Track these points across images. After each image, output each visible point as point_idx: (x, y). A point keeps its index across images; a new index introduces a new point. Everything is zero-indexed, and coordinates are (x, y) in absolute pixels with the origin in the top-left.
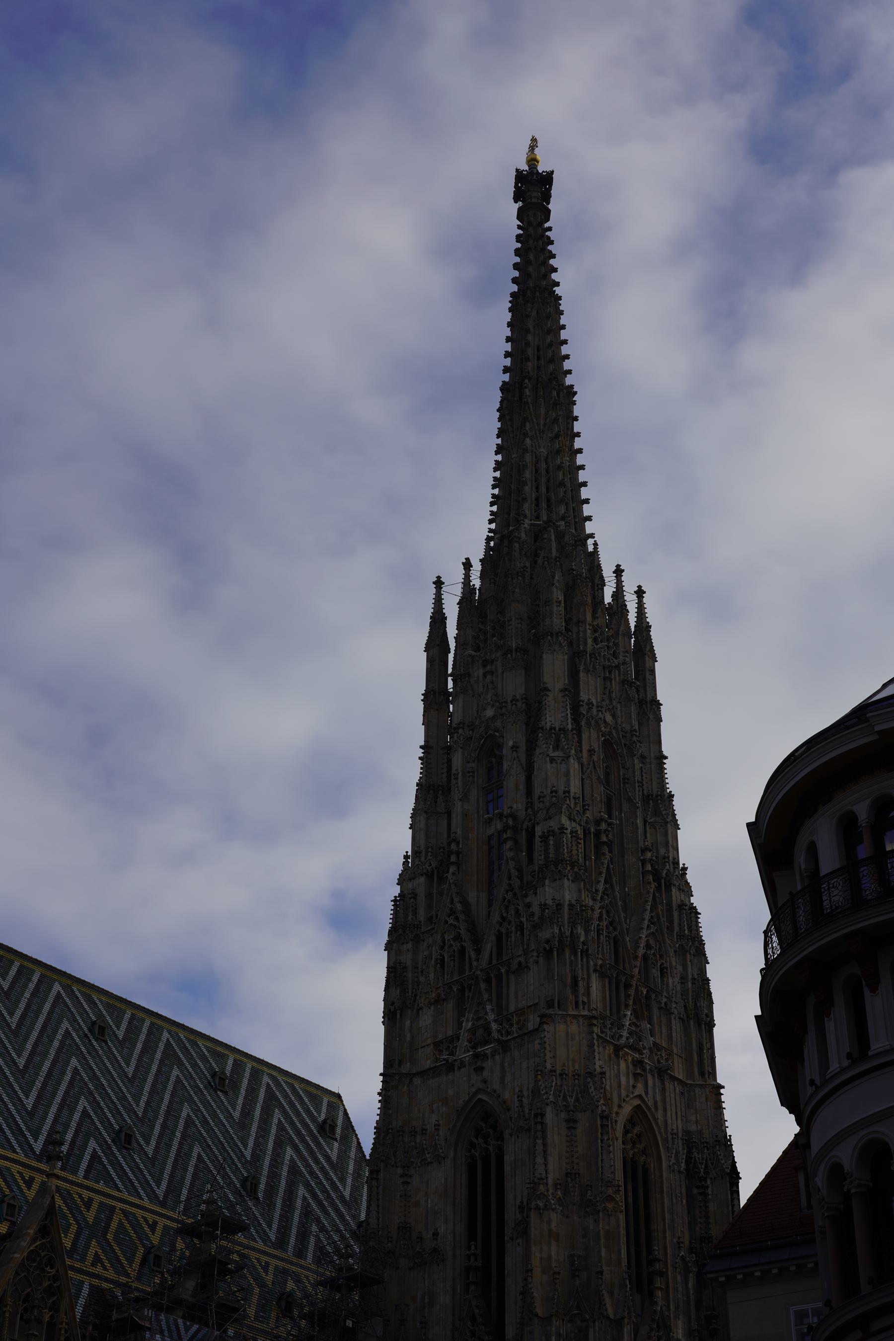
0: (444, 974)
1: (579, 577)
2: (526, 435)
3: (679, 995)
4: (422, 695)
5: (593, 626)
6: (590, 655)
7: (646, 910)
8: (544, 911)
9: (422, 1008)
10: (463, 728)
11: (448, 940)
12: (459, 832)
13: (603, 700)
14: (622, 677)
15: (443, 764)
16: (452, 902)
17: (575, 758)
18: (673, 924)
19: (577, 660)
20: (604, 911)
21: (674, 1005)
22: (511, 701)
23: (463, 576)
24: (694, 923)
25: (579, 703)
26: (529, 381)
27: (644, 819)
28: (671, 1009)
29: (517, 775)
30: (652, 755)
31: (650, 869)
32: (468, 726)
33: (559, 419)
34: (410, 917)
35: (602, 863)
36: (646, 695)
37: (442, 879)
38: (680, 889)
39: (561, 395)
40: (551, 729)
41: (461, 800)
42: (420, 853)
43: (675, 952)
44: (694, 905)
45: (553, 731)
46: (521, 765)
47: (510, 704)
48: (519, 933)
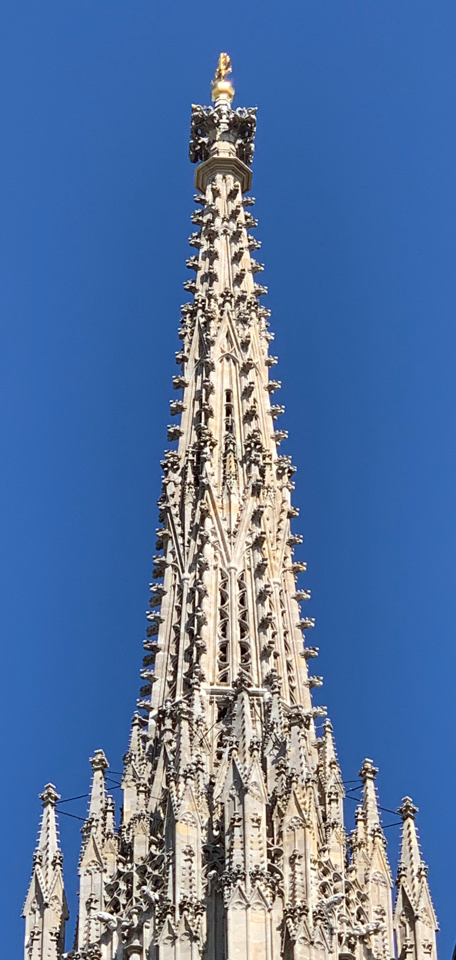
2: (205, 540)
19: (291, 923)
26: (211, 450)
33: (262, 512)
39: (267, 473)
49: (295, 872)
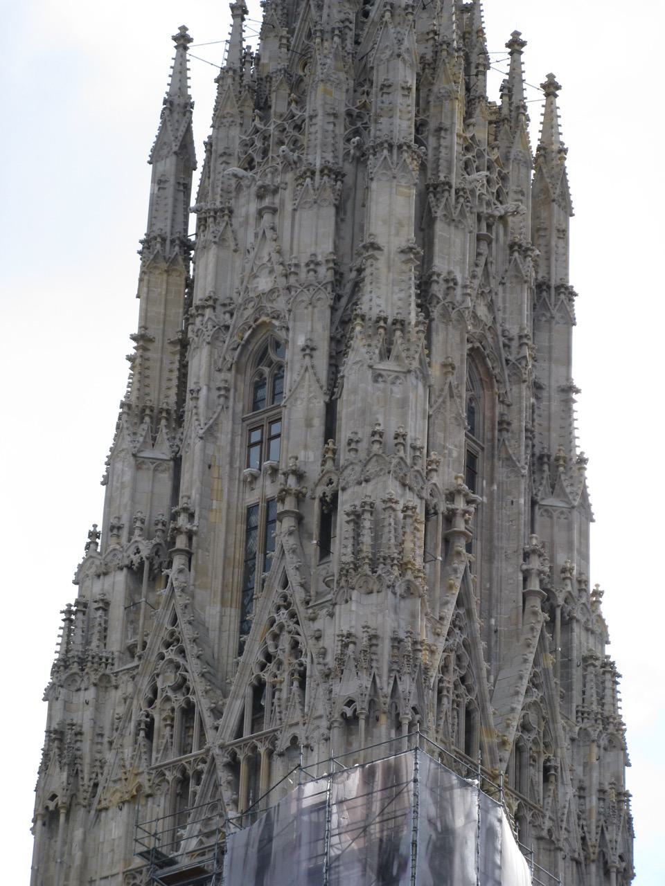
0: (151, 751)
1: (445, 47)
3: (574, 818)
4: (141, 242)
5: (465, 139)
6: (457, 192)
7: (525, 661)
8: (346, 646)
9: (106, 809)
10: (214, 308)
11: (163, 690)
12: (195, 495)
13: (474, 277)
14: (510, 238)
15: (171, 371)
16: (174, 621)
17: (420, 375)
18: (572, 690)
19: (433, 199)
20: (453, 656)
21: (563, 834)
22: (307, 265)
23: (230, 30)
24: (608, 692)
25: (430, 276)
27: (532, 497)
28: (558, 840)
29: (309, 400)
30: (554, 385)
31: (537, 588)
32: (224, 305)
34: (95, 643)
35: (455, 570)
36: (549, 273)
37: (156, 577)
38: (587, 630)
40: (379, 319)
41: (201, 438)
42: (119, 528)
43: (573, 740)
44: (611, 660)
45: (382, 323)
46: (318, 381)
47: (304, 269)
48: (296, 684)
49: (440, 145)
